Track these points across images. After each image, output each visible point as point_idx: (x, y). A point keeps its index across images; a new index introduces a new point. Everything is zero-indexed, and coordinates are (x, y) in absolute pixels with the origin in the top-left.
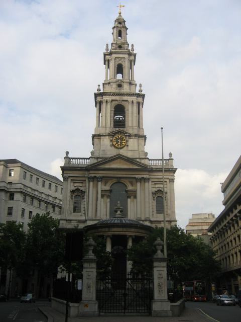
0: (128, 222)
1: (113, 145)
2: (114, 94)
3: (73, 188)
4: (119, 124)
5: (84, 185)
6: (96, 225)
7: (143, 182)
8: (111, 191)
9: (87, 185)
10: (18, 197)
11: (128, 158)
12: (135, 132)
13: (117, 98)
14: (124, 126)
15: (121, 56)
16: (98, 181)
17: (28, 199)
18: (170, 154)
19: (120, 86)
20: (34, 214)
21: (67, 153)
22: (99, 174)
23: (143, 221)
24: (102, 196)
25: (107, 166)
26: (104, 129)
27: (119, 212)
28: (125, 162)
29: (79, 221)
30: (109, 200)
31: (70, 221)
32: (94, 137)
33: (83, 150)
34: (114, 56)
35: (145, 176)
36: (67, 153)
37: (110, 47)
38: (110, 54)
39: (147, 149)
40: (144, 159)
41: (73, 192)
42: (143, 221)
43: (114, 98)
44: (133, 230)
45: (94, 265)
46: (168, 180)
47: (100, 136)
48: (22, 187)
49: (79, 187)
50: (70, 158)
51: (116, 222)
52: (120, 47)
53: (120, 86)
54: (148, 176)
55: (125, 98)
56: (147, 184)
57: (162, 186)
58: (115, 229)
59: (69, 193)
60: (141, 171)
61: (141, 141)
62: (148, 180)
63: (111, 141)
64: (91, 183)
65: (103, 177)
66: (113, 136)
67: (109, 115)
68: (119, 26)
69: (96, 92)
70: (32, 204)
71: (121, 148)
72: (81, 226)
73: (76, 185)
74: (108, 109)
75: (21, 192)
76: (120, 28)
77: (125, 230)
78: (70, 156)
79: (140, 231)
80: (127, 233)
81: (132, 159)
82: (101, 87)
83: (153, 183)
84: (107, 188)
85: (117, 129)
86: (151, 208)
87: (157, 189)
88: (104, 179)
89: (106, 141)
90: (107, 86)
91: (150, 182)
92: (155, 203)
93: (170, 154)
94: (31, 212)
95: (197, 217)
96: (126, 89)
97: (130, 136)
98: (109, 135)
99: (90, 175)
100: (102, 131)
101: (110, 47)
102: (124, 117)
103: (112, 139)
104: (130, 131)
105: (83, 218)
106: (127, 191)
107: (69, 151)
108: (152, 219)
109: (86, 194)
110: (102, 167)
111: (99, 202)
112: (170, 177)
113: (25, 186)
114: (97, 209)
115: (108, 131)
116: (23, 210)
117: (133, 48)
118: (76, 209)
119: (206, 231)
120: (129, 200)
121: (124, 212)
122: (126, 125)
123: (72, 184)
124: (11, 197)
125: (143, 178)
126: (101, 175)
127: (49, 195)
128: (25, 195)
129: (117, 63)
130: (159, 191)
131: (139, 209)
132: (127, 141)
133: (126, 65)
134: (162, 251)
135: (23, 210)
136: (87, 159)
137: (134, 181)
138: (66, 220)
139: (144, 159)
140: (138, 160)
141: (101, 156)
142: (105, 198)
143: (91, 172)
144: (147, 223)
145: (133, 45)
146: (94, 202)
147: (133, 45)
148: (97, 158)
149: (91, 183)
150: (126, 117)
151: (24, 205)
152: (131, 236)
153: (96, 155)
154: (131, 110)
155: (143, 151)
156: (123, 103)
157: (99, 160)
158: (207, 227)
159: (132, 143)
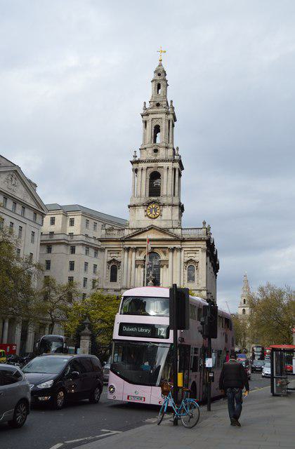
1: (147, 215)
2: (149, 161)
3: (110, 259)
4: (154, 191)
10: (79, 250)
12: (169, 200)
13: (153, 164)
15: (158, 116)
16: (130, 252)
18: (204, 223)
19: (156, 151)
24: (137, 266)
25: (141, 237)
29: (115, 290)
31: (107, 289)
34: (151, 116)
35: (177, 246)
37: (148, 106)
38: (147, 115)
41: (109, 262)
43: (149, 165)
48: (84, 238)
49: (116, 258)
52: (158, 105)
53: (156, 151)
54: (179, 246)
55: (160, 164)
57: (193, 255)
59: (106, 264)
62: (181, 249)
63: (146, 211)
64: (126, 254)
66: (148, 206)
67: (144, 183)
68: (158, 78)
69: (132, 159)
71: (155, 218)
73: (112, 255)
75: (83, 245)
76: (160, 80)
81: (168, 229)
82: (138, 152)
83: (186, 252)
84: (141, 258)
86: (182, 277)
87: (189, 259)
89: (141, 212)
90: (144, 152)
92: (186, 273)
93: (204, 223)
96: (162, 153)
97: (164, 205)
99: (125, 246)
100: (137, 201)
101: (148, 106)
110: (136, 238)
111: (133, 272)
112: (202, 246)
115: (143, 201)
116: (86, 264)
117: (171, 105)
118: (113, 278)
120: (161, 269)
123: (109, 255)
124: (73, 251)
125: (175, 248)
126: (135, 246)
128: (87, 247)
129: (155, 124)
130: (191, 260)
133: (163, 126)
135: (86, 264)
140: (171, 230)
143: (126, 243)
145: (172, 101)
147: (172, 101)
151: (87, 259)
156: (159, 170)
157: (134, 231)
159: (166, 212)
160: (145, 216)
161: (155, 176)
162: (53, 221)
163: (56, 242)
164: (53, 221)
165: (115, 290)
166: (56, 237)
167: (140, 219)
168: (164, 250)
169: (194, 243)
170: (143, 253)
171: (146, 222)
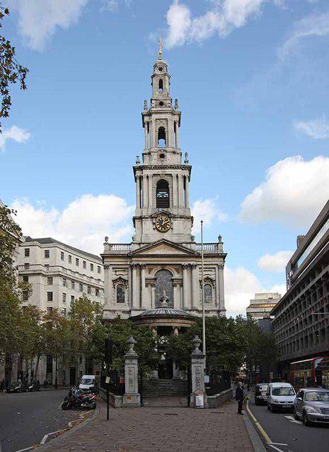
0: (173, 313)
4: (163, 203)
5: (126, 273)
6: (140, 316)
7: (189, 268)
8: (155, 279)
9: (130, 273)
11: (172, 243)
12: (181, 212)
14: (168, 207)
16: (141, 269)
17: (69, 282)
18: (220, 238)
20: (77, 298)
21: (106, 238)
22: (142, 261)
23: (190, 311)
24: (147, 285)
25: (150, 253)
26: (146, 210)
27: (165, 302)
28: (170, 248)
29: (124, 312)
30: (153, 289)
32: (134, 219)
33: (124, 235)
35: (192, 263)
36: (106, 238)
39: (195, 231)
40: (190, 243)
41: (114, 281)
42: (190, 311)
44: (179, 321)
45: (136, 362)
46: (215, 266)
47: (141, 218)
49: (122, 276)
50: (111, 245)
51: (161, 313)
54: (195, 263)
56: (194, 271)
58: (160, 321)
60: (187, 255)
61: (188, 223)
63: (154, 224)
65: (147, 264)
67: (151, 192)
70: (73, 288)
71: (167, 231)
72: (125, 317)
73: (118, 273)
74: (150, 187)
77: (170, 321)
78: (109, 242)
79: (187, 322)
80: (172, 324)
84: (152, 276)
85: (160, 210)
88: (150, 267)
89: (148, 225)
91: (198, 268)
93: (220, 238)
94: (73, 297)
95: (260, 298)
97: (175, 217)
98: (151, 217)
102: (168, 192)
103: (154, 221)
104: (174, 211)
105: (128, 309)
106: (172, 280)
107: (108, 236)
108: (200, 309)
109: (130, 283)
111: (143, 291)
113: (63, 268)
114: (144, 300)
115: (150, 213)
118: (120, 299)
119: (268, 314)
121: (170, 302)
122: (171, 204)
126: (144, 263)
127: (92, 278)
130: (207, 278)
131: (188, 298)
132: (172, 223)
134: (201, 348)
136: (128, 245)
137: (180, 269)
138: (110, 311)
139: (190, 243)
141: (143, 241)
142: (150, 286)
143: (133, 259)
144: (195, 314)
146: (138, 291)
148: (139, 244)
149: (135, 272)
150: (171, 195)
151: (64, 290)
152: (176, 327)
153: (138, 240)
154: (175, 186)
155: (190, 235)
157: (142, 246)
158: (270, 310)
159: (177, 225)
160: (154, 229)
161: (163, 185)
162: (27, 253)
163: (32, 272)
164: (27, 253)
165: (124, 312)
166: (31, 268)
167: (150, 233)
168: (176, 267)
169: (210, 259)
170: (153, 271)
171: (155, 236)
